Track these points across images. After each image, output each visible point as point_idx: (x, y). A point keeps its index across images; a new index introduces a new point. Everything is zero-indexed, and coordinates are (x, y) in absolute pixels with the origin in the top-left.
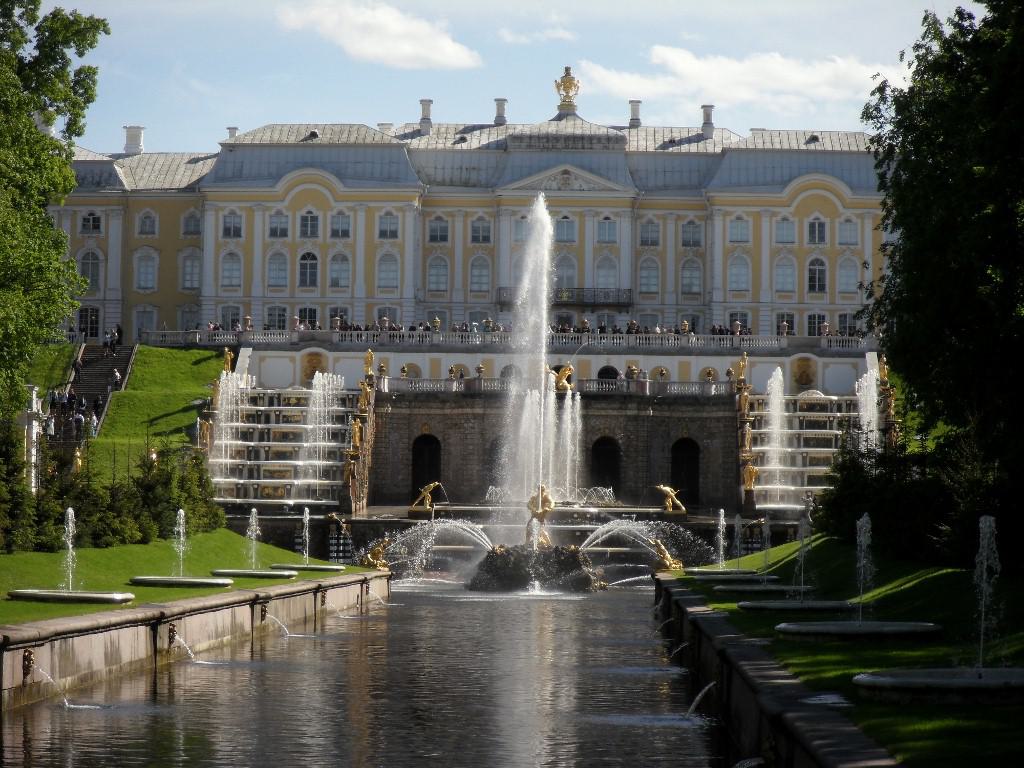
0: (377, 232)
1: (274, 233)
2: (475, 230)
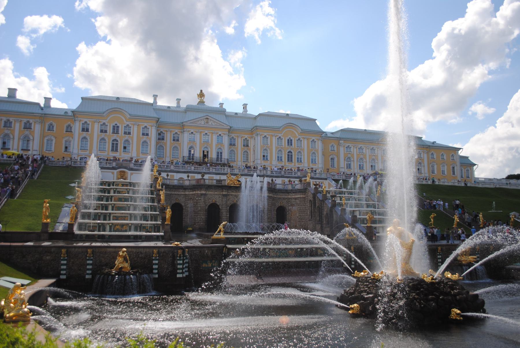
0: (141, 134)
1: (102, 131)
2: (174, 137)
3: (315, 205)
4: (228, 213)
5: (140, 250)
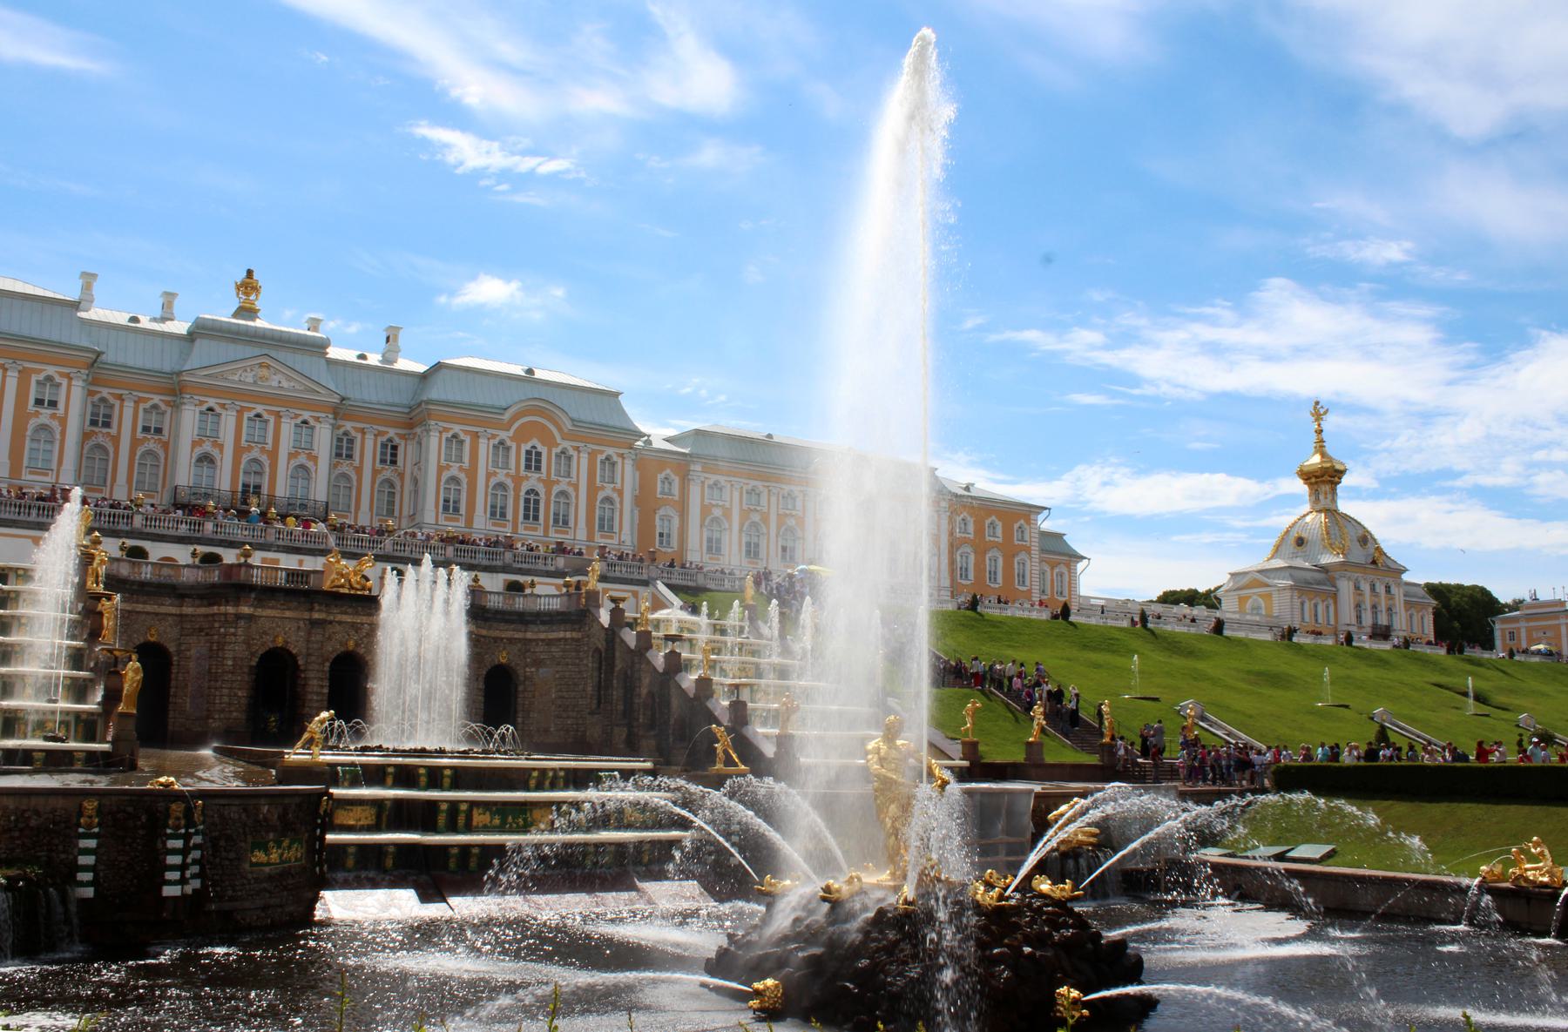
0: (32, 401)
3: (612, 665)
4: (326, 683)
5: (34, 801)
